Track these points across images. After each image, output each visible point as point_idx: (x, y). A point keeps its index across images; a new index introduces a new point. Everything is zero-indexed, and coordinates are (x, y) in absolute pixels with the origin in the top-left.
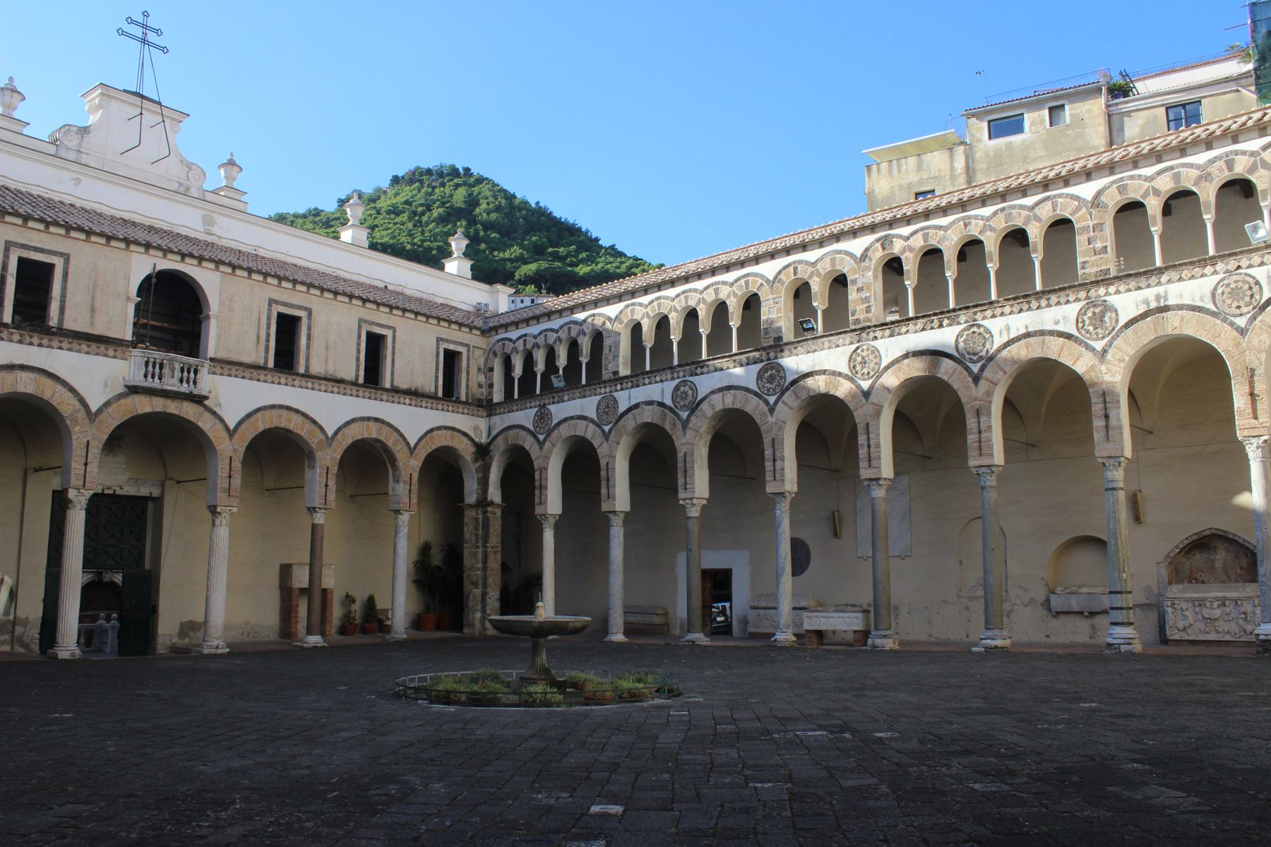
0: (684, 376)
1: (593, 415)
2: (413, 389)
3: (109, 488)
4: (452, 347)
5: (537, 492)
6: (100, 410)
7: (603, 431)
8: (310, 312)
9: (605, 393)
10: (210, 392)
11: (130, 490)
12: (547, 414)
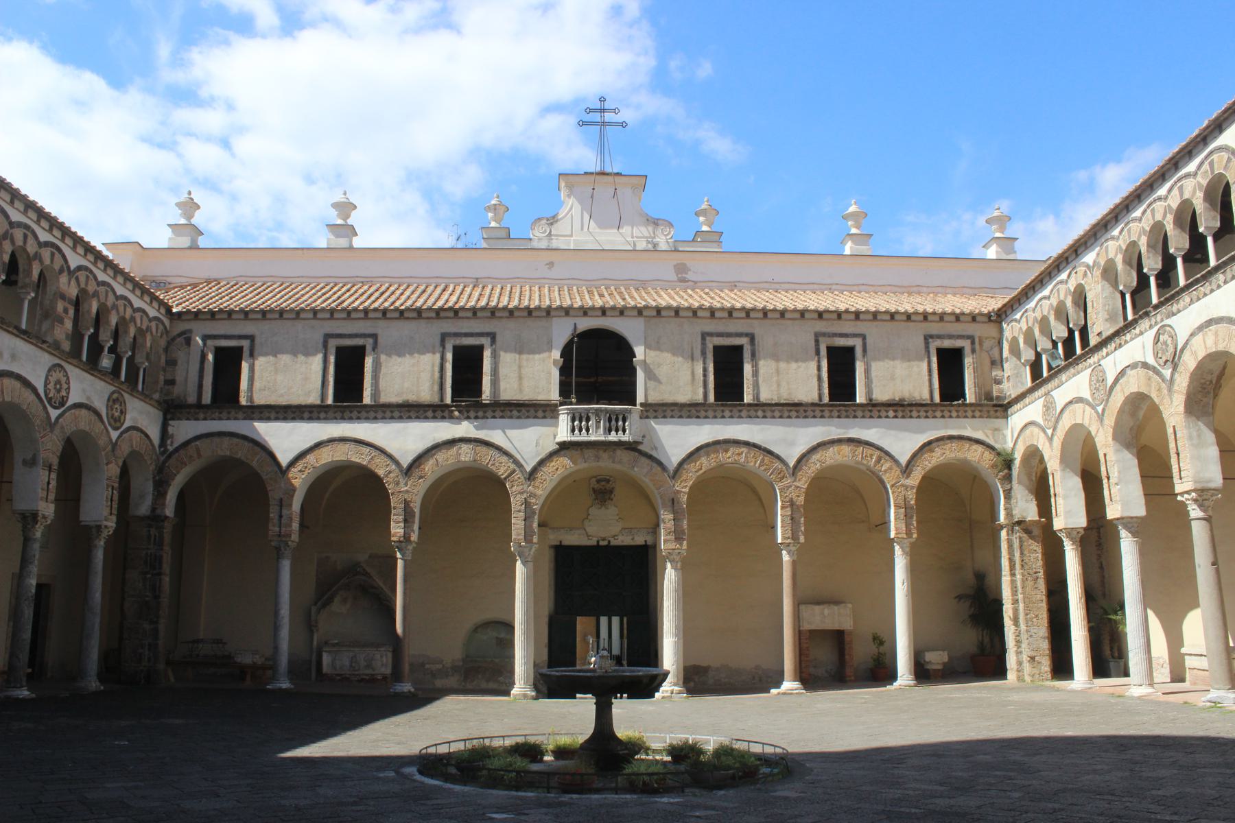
0: (1162, 320)
1: (1087, 395)
2: (897, 399)
3: (604, 539)
4: (947, 344)
5: (1053, 500)
6: (535, 470)
7: (1097, 412)
8: (752, 338)
9: (1095, 363)
10: (644, 437)
11: (625, 540)
12: (1052, 403)
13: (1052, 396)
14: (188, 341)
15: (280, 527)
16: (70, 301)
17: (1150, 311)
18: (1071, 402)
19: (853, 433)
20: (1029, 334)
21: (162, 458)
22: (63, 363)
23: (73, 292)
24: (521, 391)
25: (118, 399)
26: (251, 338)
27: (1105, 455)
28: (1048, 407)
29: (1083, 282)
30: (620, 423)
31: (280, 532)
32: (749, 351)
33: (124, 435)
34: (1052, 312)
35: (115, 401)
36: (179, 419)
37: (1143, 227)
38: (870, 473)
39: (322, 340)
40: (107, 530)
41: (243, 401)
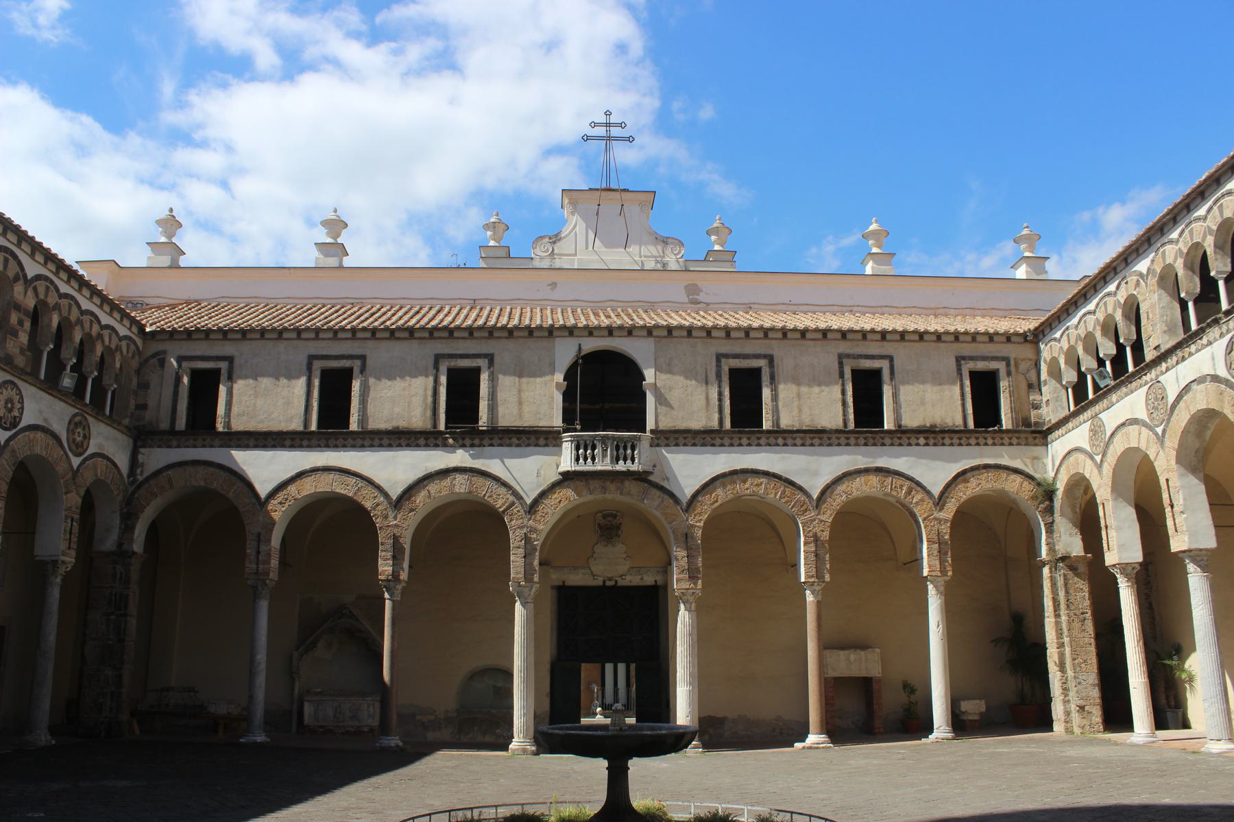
1: (1142, 414)
2: (928, 425)
3: (610, 579)
4: (981, 366)
5: (1104, 533)
6: (536, 502)
7: (1156, 434)
8: (770, 359)
9: (1152, 380)
10: (654, 466)
11: (632, 580)
12: (1100, 427)
13: (1100, 419)
14: (162, 363)
15: (257, 564)
16: (26, 313)
17: (1220, 318)
18: (1123, 424)
19: (882, 462)
20: (1089, 338)
21: (131, 489)
22: (16, 381)
23: (30, 302)
24: (521, 417)
25: (80, 422)
26: (230, 360)
27: (1167, 480)
28: (1095, 432)
29: (1135, 293)
30: (629, 451)
31: (258, 570)
32: (768, 374)
33: (87, 462)
34: (1098, 328)
35: (76, 425)
36: (151, 446)
37: (1208, 226)
38: (900, 506)
39: (305, 362)
40: (64, 566)
41: (220, 427)
